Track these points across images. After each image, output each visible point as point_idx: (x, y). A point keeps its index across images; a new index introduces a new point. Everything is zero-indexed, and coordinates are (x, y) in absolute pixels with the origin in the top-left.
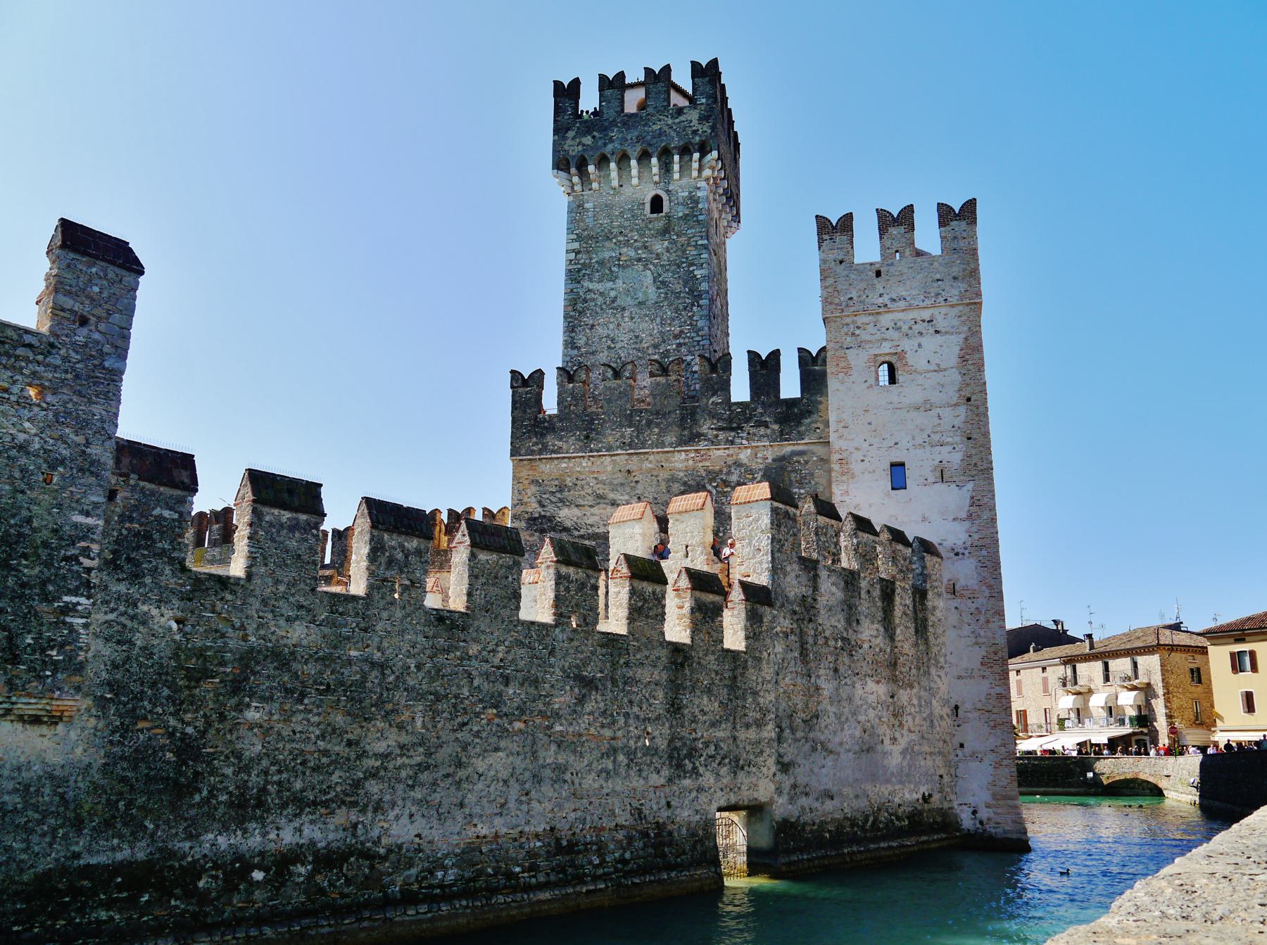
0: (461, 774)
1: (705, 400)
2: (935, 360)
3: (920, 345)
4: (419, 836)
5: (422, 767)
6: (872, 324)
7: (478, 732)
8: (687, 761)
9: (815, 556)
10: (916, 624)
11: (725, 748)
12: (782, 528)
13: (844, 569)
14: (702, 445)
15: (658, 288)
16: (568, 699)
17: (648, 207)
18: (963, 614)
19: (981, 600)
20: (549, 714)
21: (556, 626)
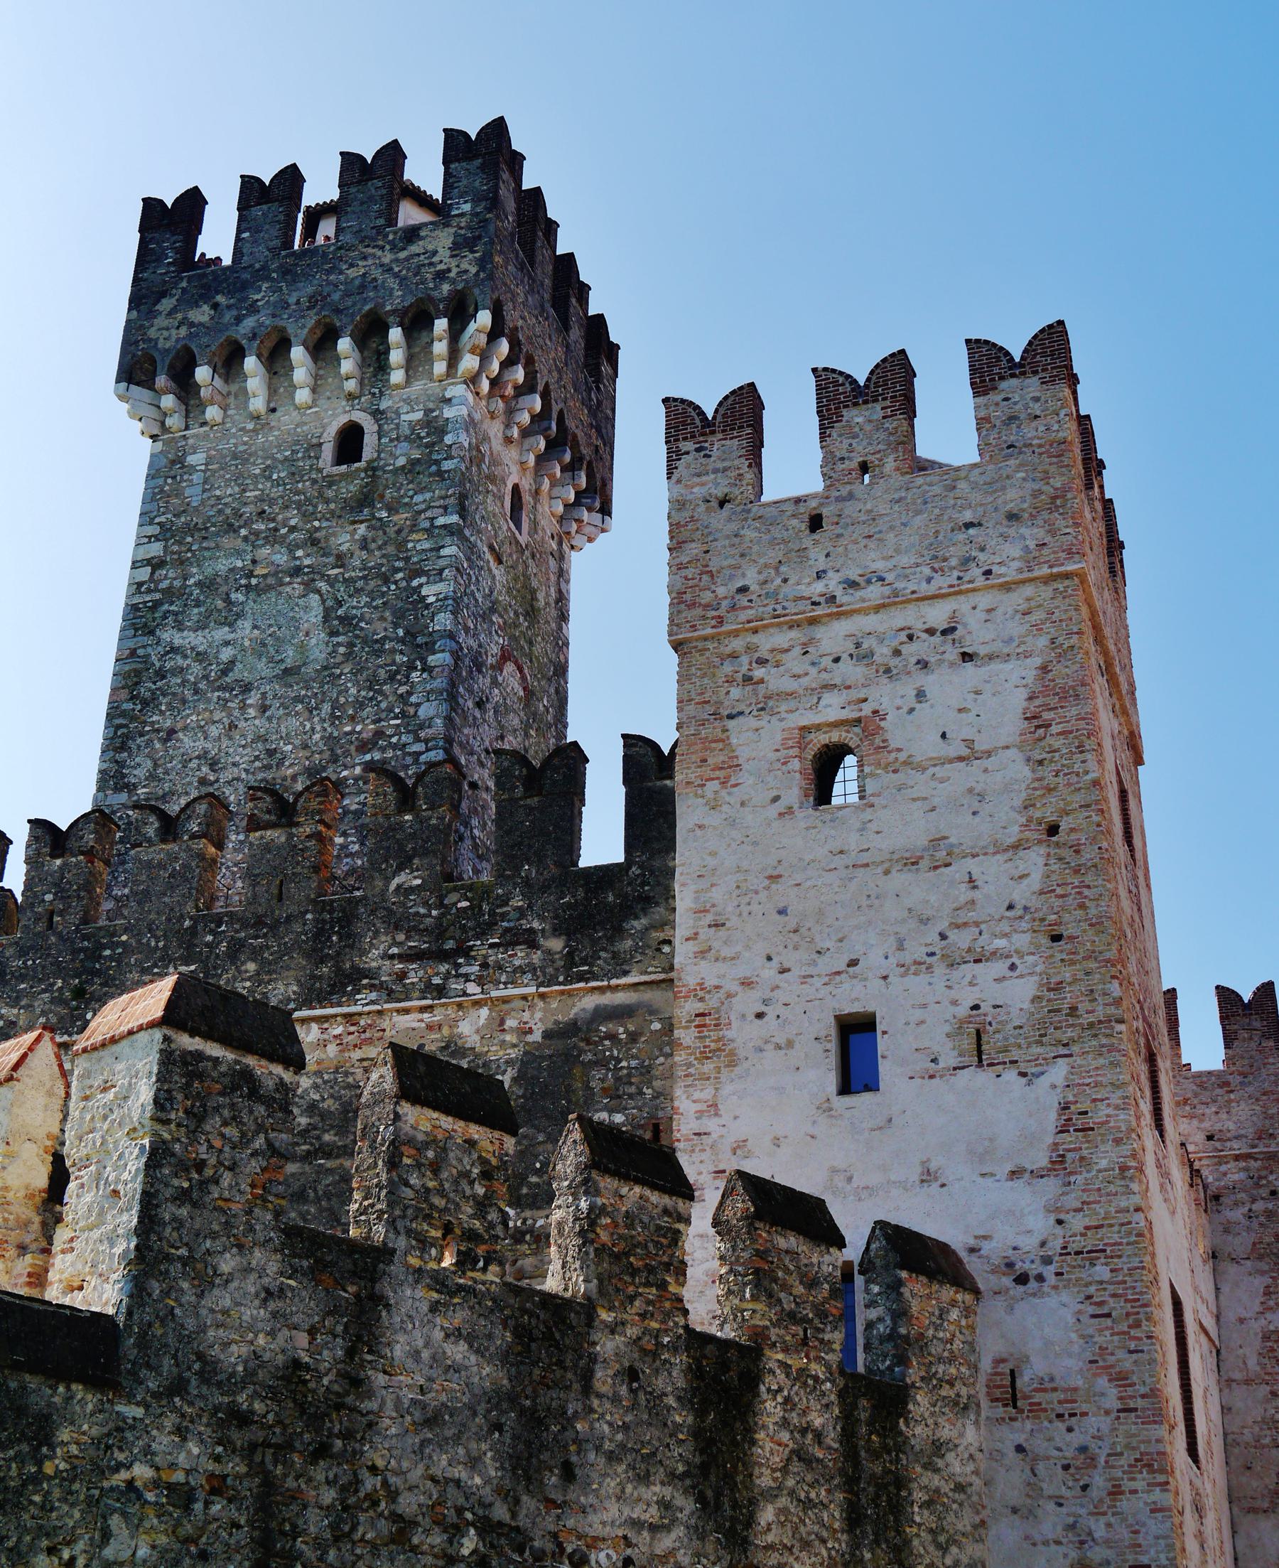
1: (379, 883)
2: (962, 729)
3: (920, 695)
6: (797, 650)
9: (380, 1232)
12: (212, 1124)
14: (364, 1003)
15: (333, 633)
17: (328, 452)
18: (1041, 1468)
19: (1096, 1422)
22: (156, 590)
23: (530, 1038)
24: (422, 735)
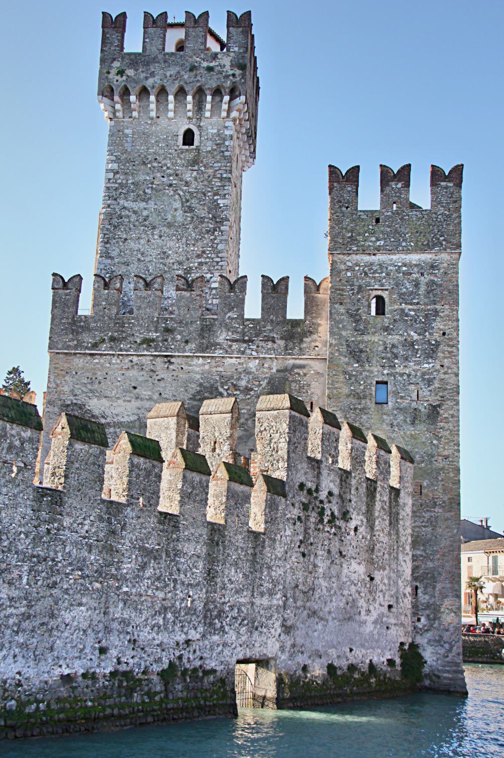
0: (53, 623)
4: (19, 673)
5: (26, 617)
7: (67, 589)
8: (217, 621)
9: (319, 456)
10: (390, 517)
11: (245, 611)
12: (297, 433)
13: (340, 469)
15: (185, 212)
16: (133, 566)
20: (119, 577)
21: (128, 506)
22: (116, 183)
23: (272, 371)
24: (220, 255)
